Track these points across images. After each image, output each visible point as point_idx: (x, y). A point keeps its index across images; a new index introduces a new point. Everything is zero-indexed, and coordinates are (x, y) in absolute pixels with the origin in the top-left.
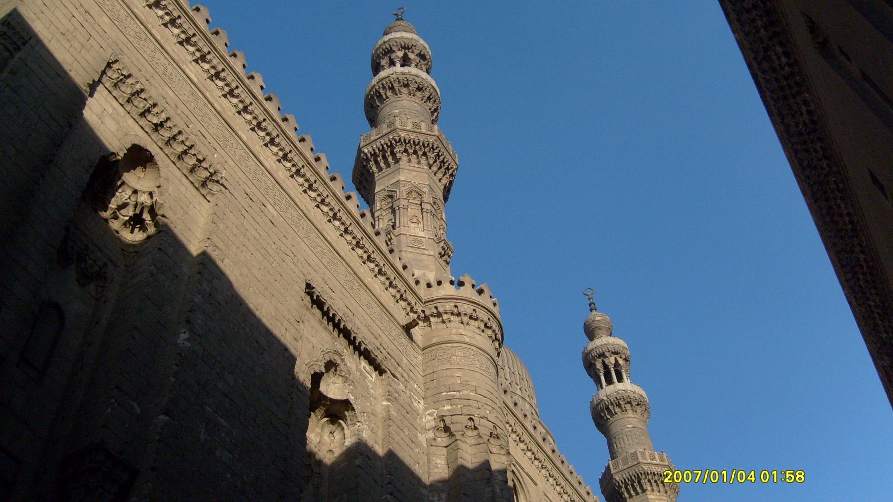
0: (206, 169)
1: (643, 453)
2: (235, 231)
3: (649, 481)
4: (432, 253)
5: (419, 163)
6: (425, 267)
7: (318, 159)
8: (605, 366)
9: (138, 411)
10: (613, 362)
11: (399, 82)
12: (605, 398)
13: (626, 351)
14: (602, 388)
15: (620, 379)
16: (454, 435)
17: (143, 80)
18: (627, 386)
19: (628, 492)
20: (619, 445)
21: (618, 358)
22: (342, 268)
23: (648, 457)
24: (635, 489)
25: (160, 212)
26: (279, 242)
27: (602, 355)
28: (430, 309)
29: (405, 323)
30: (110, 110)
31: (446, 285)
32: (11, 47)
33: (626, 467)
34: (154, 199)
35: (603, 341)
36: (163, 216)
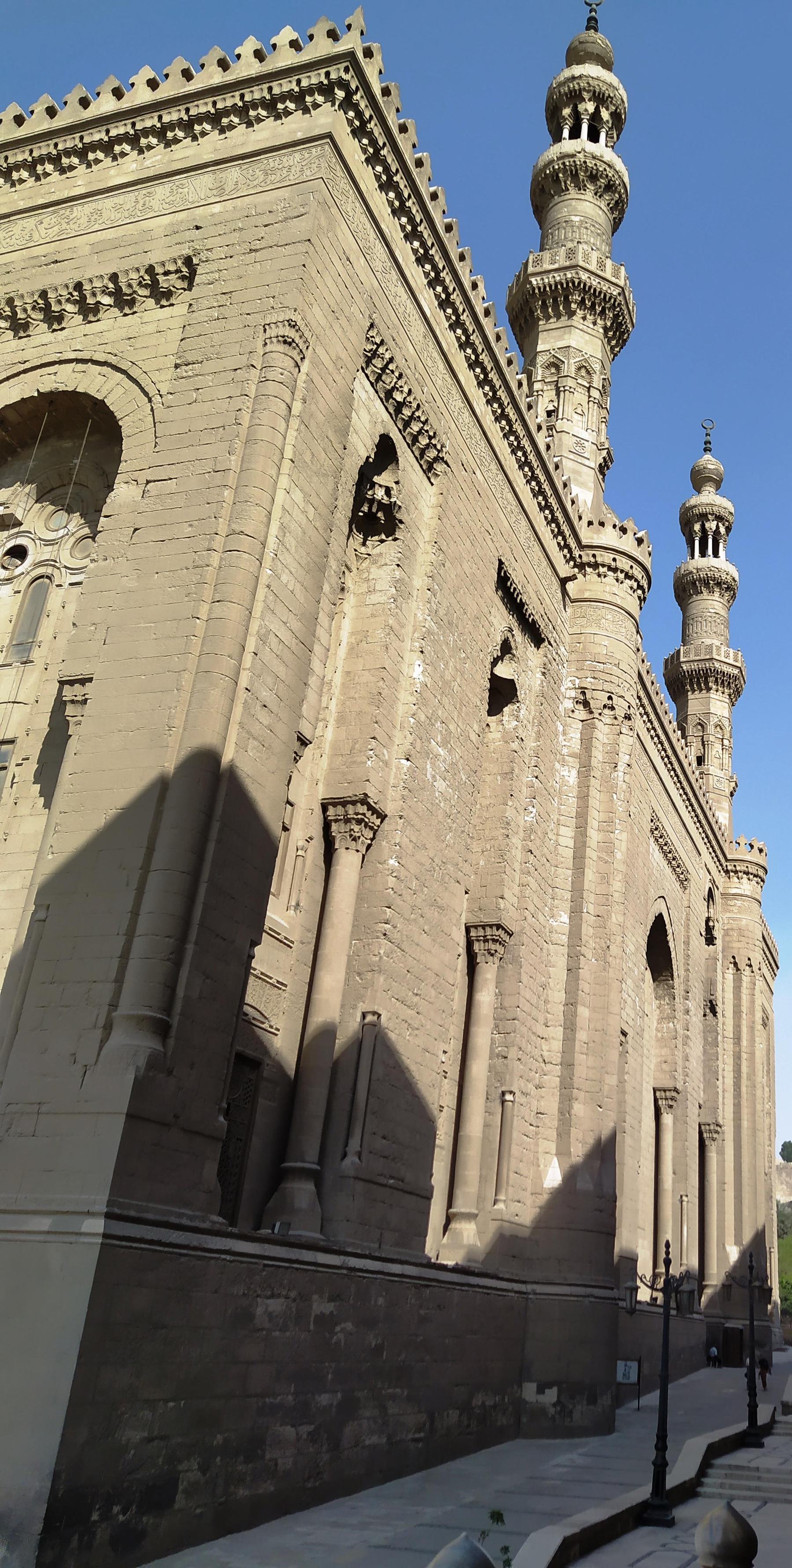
0: (435, 446)
1: (718, 648)
2: (454, 521)
3: (717, 679)
4: (592, 465)
5: (595, 323)
6: (582, 485)
7: (419, 163)
8: (703, 529)
9: (387, 757)
10: (714, 528)
11: (586, 170)
12: (695, 571)
13: (730, 518)
14: (693, 557)
15: (716, 554)
16: (591, 712)
17: (391, 343)
18: (721, 564)
19: (692, 685)
20: (693, 629)
21: (720, 525)
22: (524, 522)
23: (723, 653)
24: (699, 684)
25: (398, 516)
26: (483, 519)
27: (703, 517)
28: (588, 555)
29: (563, 575)
30: (364, 396)
31: (609, 528)
32: (298, 359)
33: (698, 658)
34: (392, 500)
35: (709, 498)
36: (401, 522)
